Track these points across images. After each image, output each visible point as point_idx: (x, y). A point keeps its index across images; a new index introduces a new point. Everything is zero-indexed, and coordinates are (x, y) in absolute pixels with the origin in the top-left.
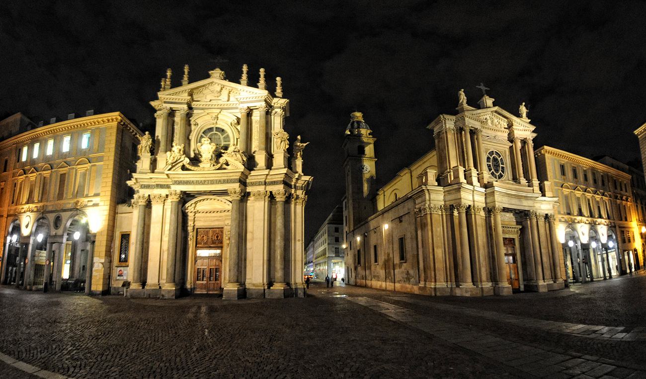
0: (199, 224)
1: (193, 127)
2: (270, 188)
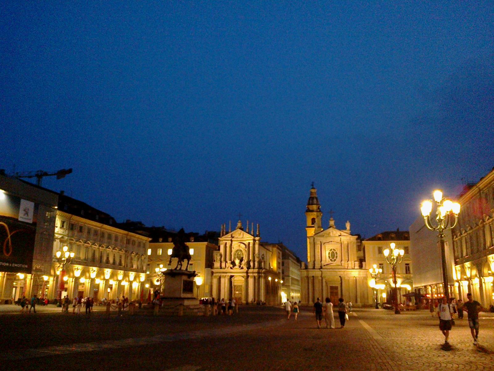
0: (235, 284)
1: (233, 249)
2: (254, 274)
